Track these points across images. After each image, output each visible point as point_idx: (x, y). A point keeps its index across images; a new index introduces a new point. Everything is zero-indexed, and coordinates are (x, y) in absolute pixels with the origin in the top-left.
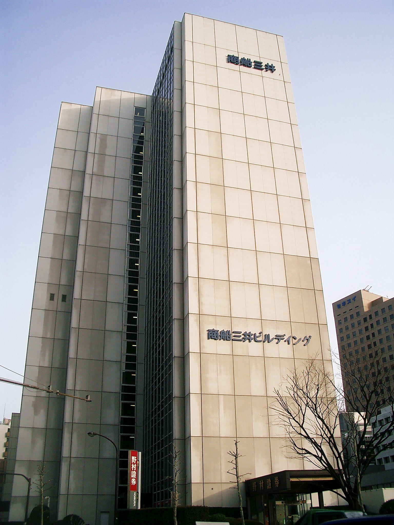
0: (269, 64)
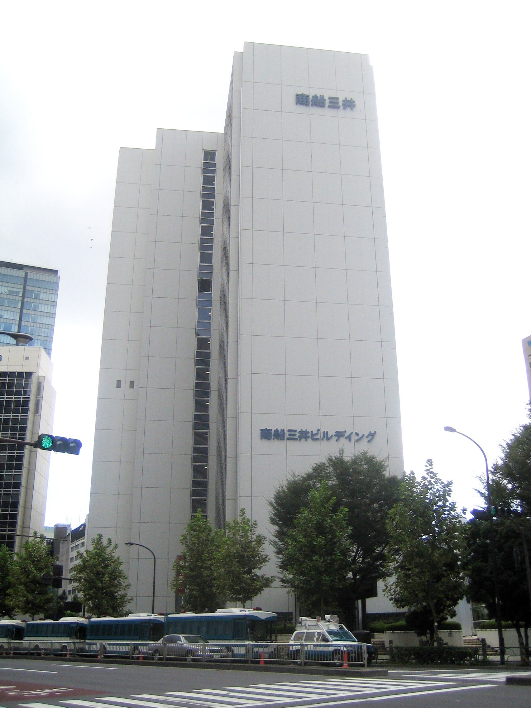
0: (348, 99)
